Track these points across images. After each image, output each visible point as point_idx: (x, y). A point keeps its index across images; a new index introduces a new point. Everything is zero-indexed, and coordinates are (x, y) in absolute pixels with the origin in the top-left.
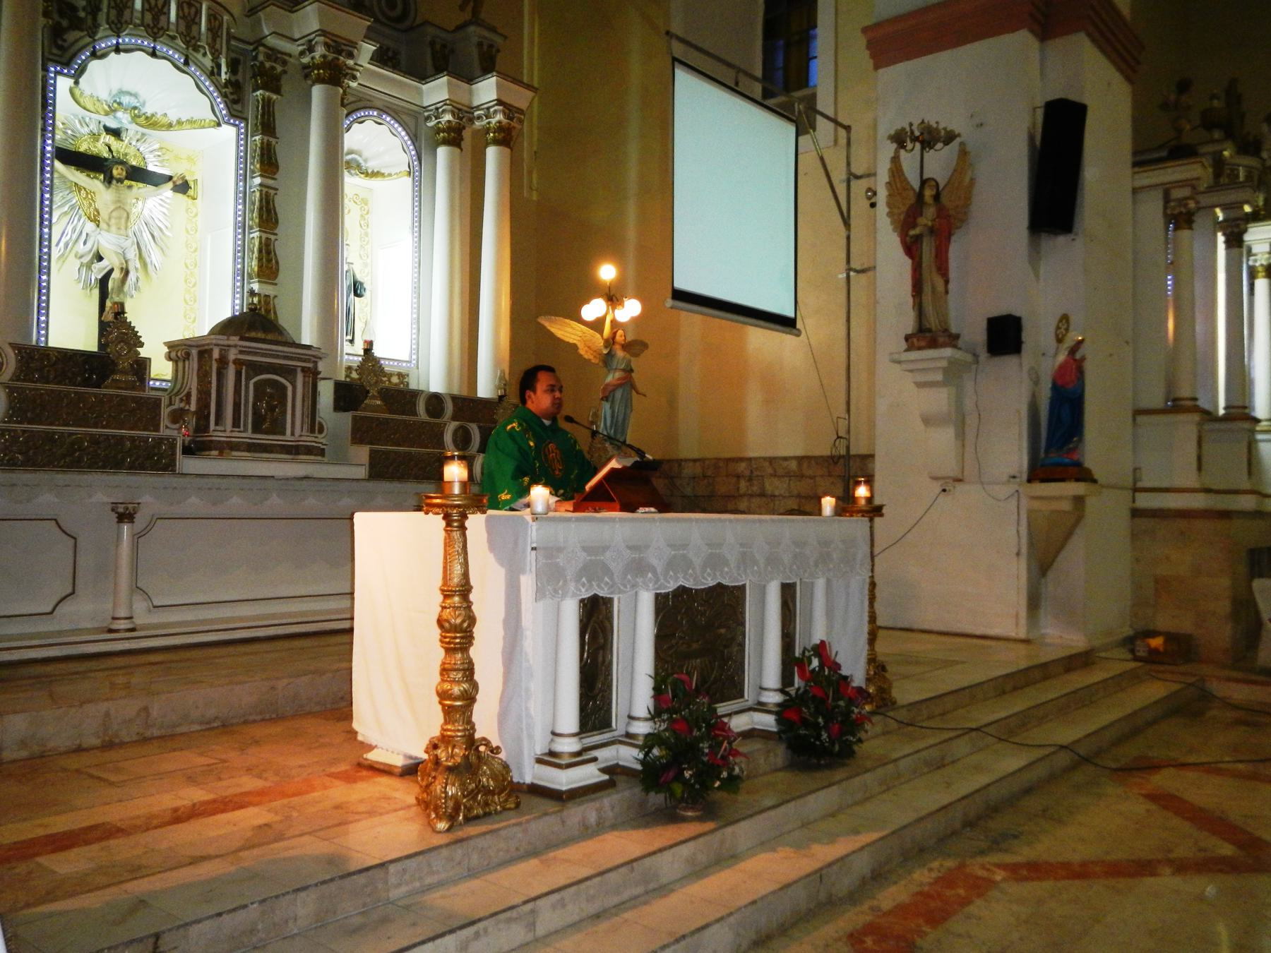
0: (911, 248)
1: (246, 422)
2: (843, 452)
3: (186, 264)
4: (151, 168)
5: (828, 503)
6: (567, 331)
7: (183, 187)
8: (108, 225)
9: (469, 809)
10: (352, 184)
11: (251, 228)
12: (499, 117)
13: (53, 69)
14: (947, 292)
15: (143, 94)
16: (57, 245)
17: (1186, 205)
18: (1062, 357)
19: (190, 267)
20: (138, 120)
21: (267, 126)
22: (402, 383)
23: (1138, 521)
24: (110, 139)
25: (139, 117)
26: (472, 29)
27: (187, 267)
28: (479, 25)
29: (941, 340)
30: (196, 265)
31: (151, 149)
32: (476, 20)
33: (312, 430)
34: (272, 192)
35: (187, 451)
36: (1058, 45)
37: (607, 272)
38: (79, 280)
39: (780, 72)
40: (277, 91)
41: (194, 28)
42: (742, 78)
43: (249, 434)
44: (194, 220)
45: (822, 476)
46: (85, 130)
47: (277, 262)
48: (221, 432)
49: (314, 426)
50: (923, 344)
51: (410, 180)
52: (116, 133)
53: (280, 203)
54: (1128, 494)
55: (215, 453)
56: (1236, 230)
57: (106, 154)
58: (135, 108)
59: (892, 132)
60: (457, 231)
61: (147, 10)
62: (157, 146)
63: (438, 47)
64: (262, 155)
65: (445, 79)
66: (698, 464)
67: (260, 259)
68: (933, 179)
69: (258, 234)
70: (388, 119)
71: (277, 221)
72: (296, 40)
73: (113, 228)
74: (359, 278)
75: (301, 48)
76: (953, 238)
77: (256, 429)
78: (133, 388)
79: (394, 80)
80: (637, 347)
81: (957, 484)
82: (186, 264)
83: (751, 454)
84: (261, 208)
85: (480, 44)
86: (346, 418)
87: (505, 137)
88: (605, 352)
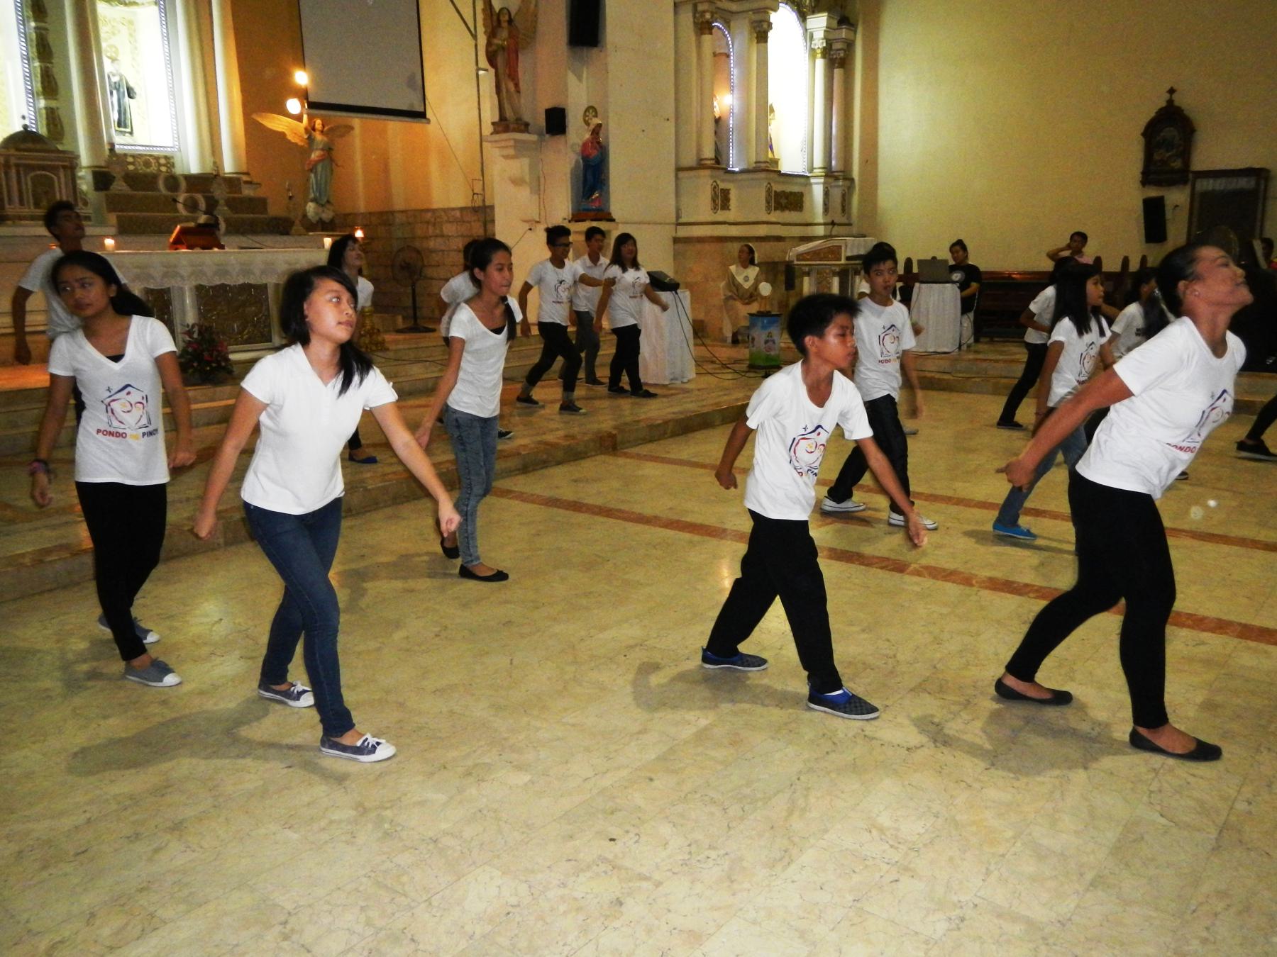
1: (28, 202)
2: (480, 204)
6: (276, 123)
14: (518, 92)
22: (168, 163)
23: (677, 246)
29: (511, 126)
34: (43, 32)
45: (474, 221)
53: (51, 39)
54: (673, 226)
55: (9, 222)
67: (42, 83)
81: (537, 225)
83: (435, 206)
86: (102, 194)
88: (306, 137)
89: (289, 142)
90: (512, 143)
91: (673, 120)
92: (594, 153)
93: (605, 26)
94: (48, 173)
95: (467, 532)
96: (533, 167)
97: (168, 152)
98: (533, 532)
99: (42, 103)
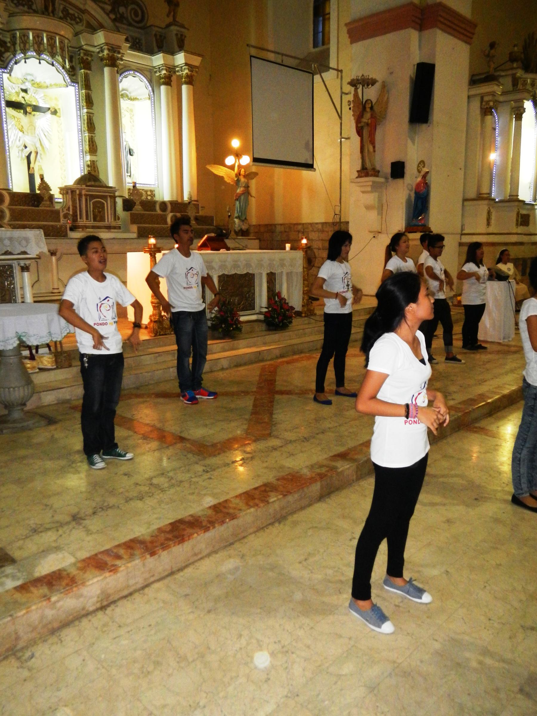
0: (359, 132)
2: (338, 220)
5: (288, 246)
6: (219, 171)
7: (55, 112)
9: (160, 332)
10: (124, 104)
11: (84, 131)
12: (186, 71)
14: (374, 151)
17: (489, 104)
18: (419, 179)
20: (34, 86)
21: (87, 86)
24: (23, 94)
25: (34, 84)
26: (173, 28)
28: (176, 25)
29: (370, 173)
32: (174, 23)
33: (115, 220)
34: (91, 115)
35: (72, 229)
36: (427, 33)
37: (236, 143)
38: (19, 157)
39: (321, 34)
40: (90, 69)
41: (54, 49)
42: (284, 57)
43: (92, 222)
46: (14, 91)
47: (96, 146)
48: (82, 222)
49: (116, 217)
50: (363, 175)
51: (150, 101)
52: (25, 91)
54: (459, 236)
55: (81, 230)
56: (519, 113)
57: (23, 102)
58: (33, 80)
59: (349, 81)
60: (172, 127)
62: (42, 95)
63: (158, 37)
64: (86, 99)
65: (161, 54)
66: (282, 226)
67: (89, 145)
68: (370, 100)
70: (138, 74)
71: (95, 128)
72: (96, 46)
74: (131, 147)
75: (98, 50)
76: (378, 127)
77: (95, 220)
78: (49, 207)
79: (139, 56)
80: (250, 176)
81: (380, 235)
84: (88, 123)
85: (177, 35)
86: (128, 213)
87: (190, 81)
88: (236, 179)
89: (225, 182)
90: (371, 183)
91: (463, 169)
92: (423, 190)
93: (433, 109)
94: (102, 201)
95: (519, 473)
96: (380, 199)
97: (152, 188)
98: (488, 454)
99: (88, 158)
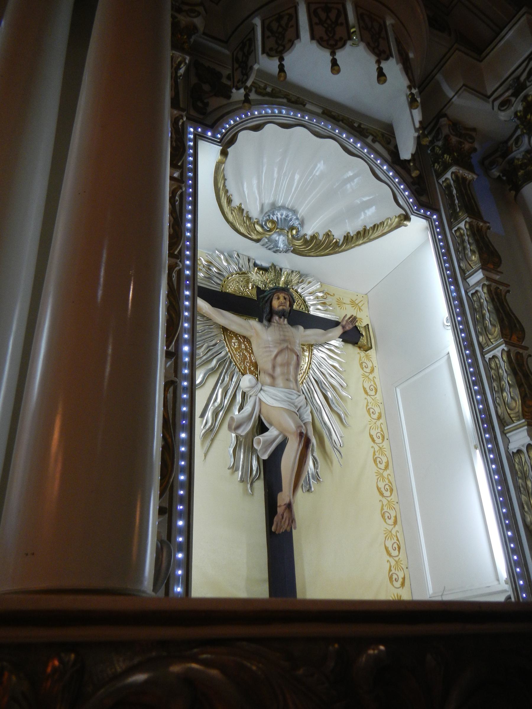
3: (371, 436)
4: (312, 313)
8: (273, 377)
13: (192, 130)
15: (302, 211)
16: (202, 415)
19: (377, 441)
27: (374, 441)
30: (383, 437)
31: (310, 290)
38: (234, 468)
44: (371, 376)
46: (234, 267)
58: (292, 228)
61: (316, 24)
62: (318, 286)
69: (503, 346)
72: (489, 97)
73: (280, 381)
82: (371, 436)
